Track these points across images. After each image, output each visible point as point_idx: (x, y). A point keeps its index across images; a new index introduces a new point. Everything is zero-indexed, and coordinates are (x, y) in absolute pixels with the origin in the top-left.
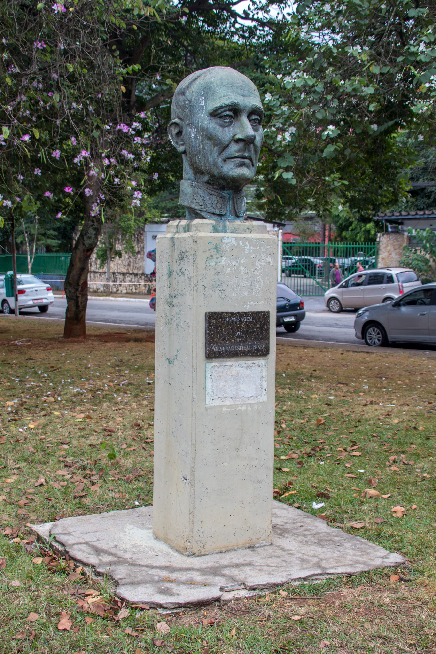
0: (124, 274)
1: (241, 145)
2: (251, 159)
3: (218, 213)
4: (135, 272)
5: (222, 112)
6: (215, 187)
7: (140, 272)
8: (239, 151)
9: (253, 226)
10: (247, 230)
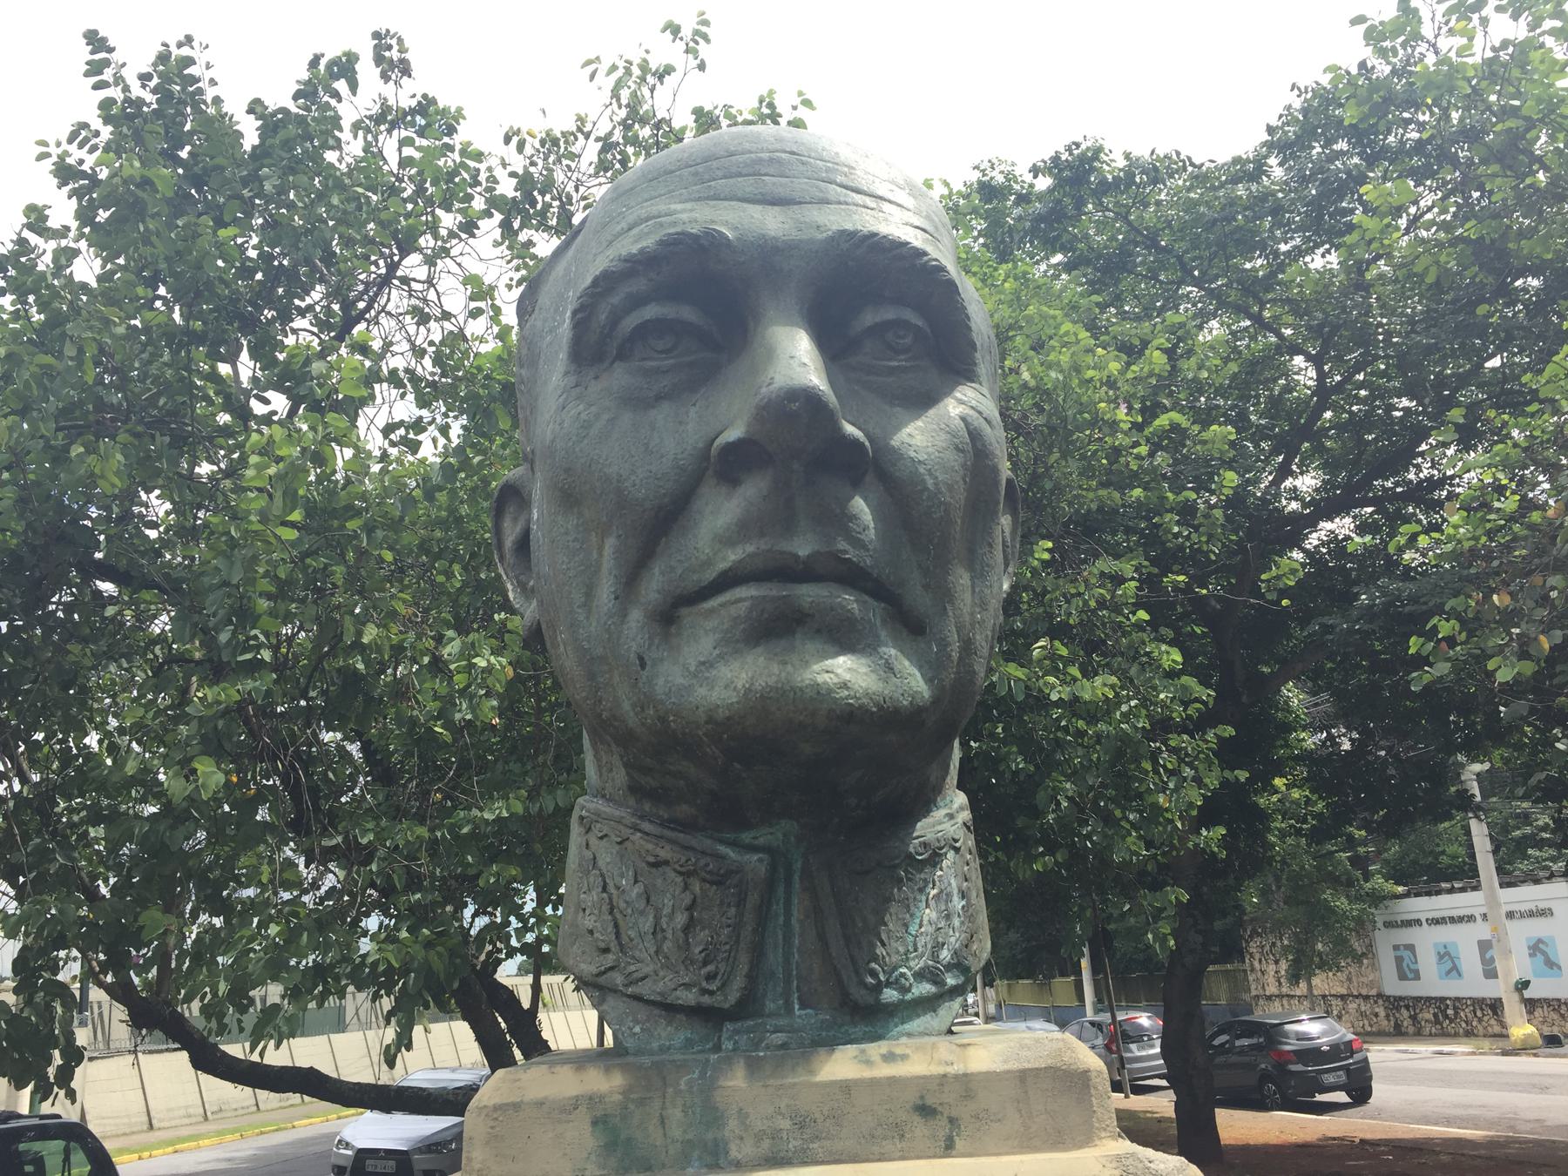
0: (1342, 997)
1: (753, 489)
2: (852, 576)
3: (689, 997)
4: (1364, 992)
5: (614, 322)
7: (1374, 992)
8: (744, 529)
9: (967, 1084)
10: (920, 1129)
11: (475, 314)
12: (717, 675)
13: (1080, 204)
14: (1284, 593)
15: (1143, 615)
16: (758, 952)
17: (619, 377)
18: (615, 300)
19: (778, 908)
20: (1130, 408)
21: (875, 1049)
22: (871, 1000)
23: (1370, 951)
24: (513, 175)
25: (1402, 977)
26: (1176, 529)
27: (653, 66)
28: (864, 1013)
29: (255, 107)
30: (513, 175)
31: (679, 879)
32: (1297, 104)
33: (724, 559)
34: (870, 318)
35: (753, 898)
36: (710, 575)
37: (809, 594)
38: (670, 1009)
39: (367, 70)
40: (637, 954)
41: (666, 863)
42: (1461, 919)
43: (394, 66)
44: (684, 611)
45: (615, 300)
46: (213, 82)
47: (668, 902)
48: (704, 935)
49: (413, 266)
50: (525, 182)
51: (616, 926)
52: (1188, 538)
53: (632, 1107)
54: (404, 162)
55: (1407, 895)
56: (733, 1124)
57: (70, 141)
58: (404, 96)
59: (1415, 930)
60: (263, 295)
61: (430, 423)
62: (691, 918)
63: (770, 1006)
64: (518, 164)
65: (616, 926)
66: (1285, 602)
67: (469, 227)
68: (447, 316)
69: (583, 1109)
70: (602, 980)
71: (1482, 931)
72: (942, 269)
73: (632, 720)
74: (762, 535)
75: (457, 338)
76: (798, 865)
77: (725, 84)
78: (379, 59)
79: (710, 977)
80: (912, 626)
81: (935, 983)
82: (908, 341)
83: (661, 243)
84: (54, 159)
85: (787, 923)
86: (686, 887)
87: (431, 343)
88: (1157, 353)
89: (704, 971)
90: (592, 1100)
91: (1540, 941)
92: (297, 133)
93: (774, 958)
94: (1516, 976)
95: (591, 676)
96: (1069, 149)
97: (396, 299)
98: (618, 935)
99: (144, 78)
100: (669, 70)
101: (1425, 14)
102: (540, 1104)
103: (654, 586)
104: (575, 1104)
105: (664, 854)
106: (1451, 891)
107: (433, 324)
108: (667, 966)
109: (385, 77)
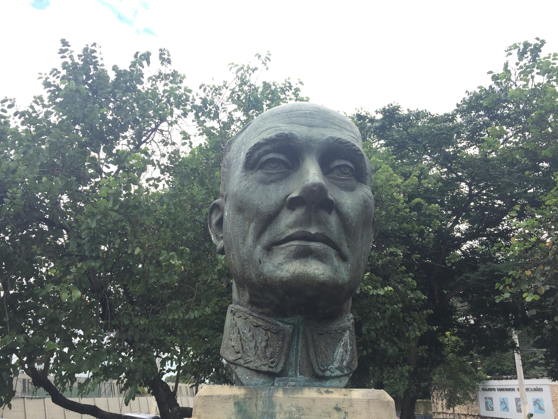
0: (465, 415)
1: (299, 212)
2: (326, 240)
3: (265, 369)
4: (473, 414)
6: (267, 310)
7: (477, 414)
8: (295, 224)
11: (184, 144)
12: (284, 267)
13: (391, 124)
14: (453, 264)
15: (404, 268)
16: (288, 356)
17: (259, 174)
18: (261, 151)
19: (295, 343)
20: (404, 195)
21: (323, 390)
22: (321, 374)
23: (476, 399)
24: (201, 98)
25: (487, 409)
26: (417, 239)
27: (251, 67)
28: (318, 378)
29: (115, 68)
30: (201, 98)
31: (264, 331)
32: (467, 97)
33: (288, 232)
34: (337, 163)
35: (287, 339)
36: (284, 237)
37: (314, 245)
38: (258, 372)
39: (155, 58)
40: (249, 354)
41: (260, 326)
42: (509, 390)
43: (165, 59)
44: (274, 247)
45: (261, 151)
46: (102, 59)
47: (260, 338)
48: (271, 349)
49: (164, 126)
50: (204, 101)
51: (242, 345)
52: (421, 242)
53: (247, 400)
54: (165, 91)
55: (491, 379)
56: (278, 408)
57: (50, 74)
58: (167, 70)
59: (493, 392)
60: (110, 131)
61: (163, 179)
62: (267, 344)
63: (290, 373)
64: (203, 95)
65: (242, 345)
66: (454, 267)
67: (185, 114)
68: (173, 144)
69: (232, 399)
70: (236, 362)
71: (517, 394)
72: (360, 150)
73: (255, 280)
74: (301, 226)
75: (176, 152)
76: (301, 330)
77: (275, 76)
78: (161, 58)
79: (272, 363)
80: (343, 258)
81: (341, 371)
82: (348, 171)
83: (277, 136)
84: (44, 79)
85: (297, 349)
86: (266, 334)
87: (168, 153)
88: (415, 177)
89: (270, 361)
90: (235, 397)
91: (537, 400)
92: (128, 79)
93: (292, 359)
94: (528, 412)
95: (243, 265)
96: (388, 106)
97: (158, 137)
98: (242, 348)
99: (80, 56)
100: (256, 69)
101: (513, 72)
102: (219, 396)
103: (266, 239)
104: (229, 397)
105: (260, 323)
106: (507, 379)
107: (169, 146)
108: (259, 358)
109: (162, 64)
